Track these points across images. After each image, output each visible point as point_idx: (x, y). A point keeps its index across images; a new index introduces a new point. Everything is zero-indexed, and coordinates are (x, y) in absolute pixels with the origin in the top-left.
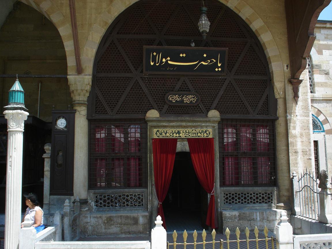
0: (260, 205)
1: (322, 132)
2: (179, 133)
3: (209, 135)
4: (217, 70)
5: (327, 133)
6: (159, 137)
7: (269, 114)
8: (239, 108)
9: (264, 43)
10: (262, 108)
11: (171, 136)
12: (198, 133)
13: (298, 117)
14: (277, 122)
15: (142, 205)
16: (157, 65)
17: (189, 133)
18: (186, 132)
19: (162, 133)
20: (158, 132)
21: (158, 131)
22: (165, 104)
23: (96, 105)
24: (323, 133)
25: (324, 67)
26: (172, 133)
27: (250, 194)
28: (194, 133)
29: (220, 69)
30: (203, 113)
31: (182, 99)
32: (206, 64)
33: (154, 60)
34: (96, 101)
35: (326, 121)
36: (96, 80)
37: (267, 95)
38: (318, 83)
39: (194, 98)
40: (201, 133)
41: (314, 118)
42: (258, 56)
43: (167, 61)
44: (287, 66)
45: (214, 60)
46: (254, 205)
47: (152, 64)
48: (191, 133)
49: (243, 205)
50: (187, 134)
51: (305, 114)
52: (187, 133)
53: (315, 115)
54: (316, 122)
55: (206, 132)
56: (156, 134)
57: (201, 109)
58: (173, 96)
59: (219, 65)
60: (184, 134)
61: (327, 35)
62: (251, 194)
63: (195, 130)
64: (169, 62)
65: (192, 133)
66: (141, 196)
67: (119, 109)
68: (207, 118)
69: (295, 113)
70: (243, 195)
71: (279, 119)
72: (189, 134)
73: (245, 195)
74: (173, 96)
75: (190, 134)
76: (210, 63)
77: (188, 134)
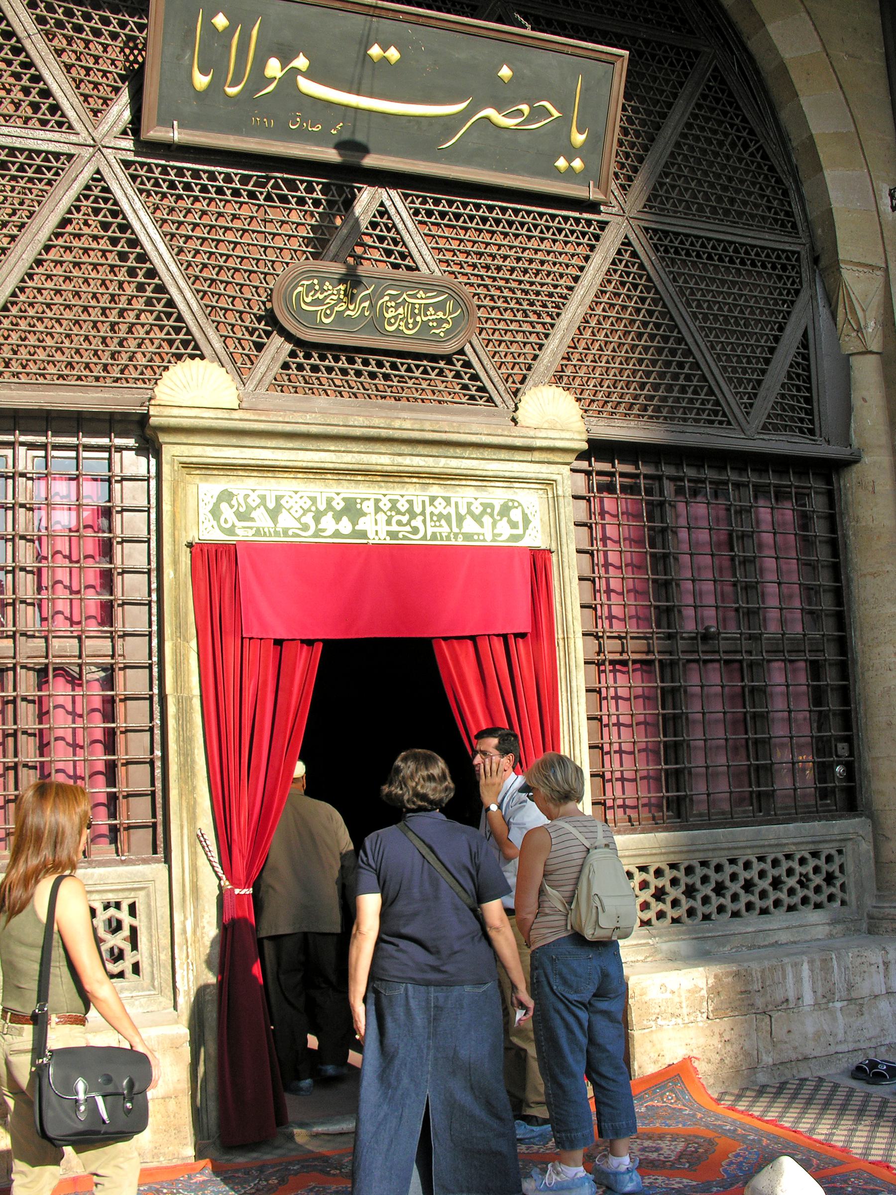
0: (793, 918)
2: (352, 510)
3: (526, 527)
4: (561, 163)
6: (231, 531)
7: (817, 431)
8: (676, 389)
9: (783, 69)
11: (306, 528)
12: (460, 519)
14: (850, 479)
15: (136, 969)
17: (413, 515)
18: (394, 507)
19: (250, 509)
20: (224, 506)
21: (226, 496)
22: (268, 334)
26: (309, 510)
27: (741, 864)
28: (440, 516)
29: (577, 164)
31: (372, 306)
39: (439, 307)
40: (478, 519)
42: (752, 132)
46: (765, 923)
48: (423, 513)
49: (709, 931)
50: (399, 523)
52: (399, 512)
55: (505, 510)
56: (215, 512)
57: (475, 377)
58: (321, 284)
59: (579, 139)
60: (382, 518)
62: (747, 866)
63: (447, 500)
64: (307, 86)
65: (432, 514)
66: (123, 915)
68: (516, 431)
70: (711, 872)
71: (866, 459)
72: (413, 523)
73: (719, 868)
74: (321, 284)
75: (417, 522)
76: (529, 120)
77: (405, 519)
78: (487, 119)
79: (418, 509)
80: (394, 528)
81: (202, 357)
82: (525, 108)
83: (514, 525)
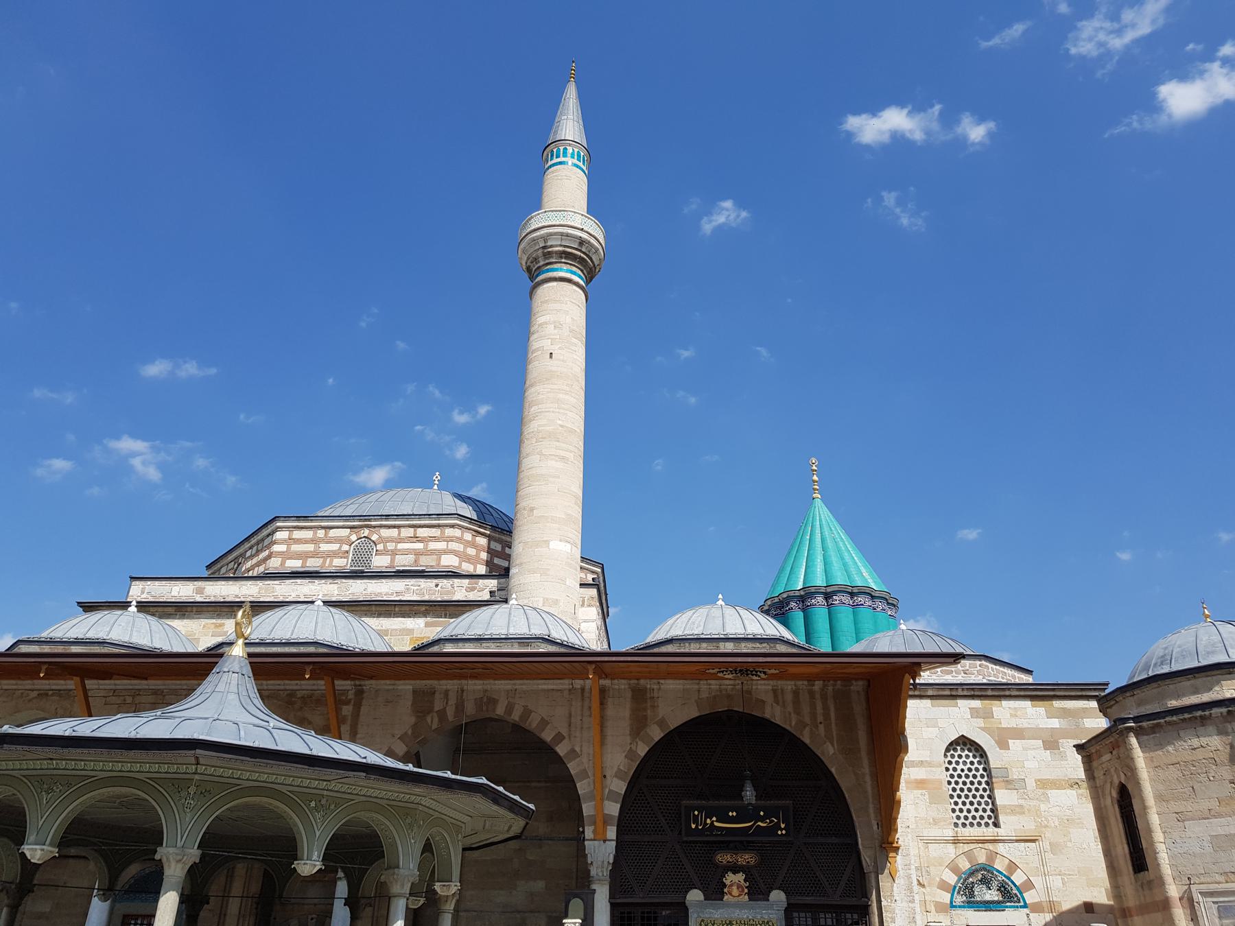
1: (1021, 907)
5: (1032, 912)
16: (700, 828)
21: (703, 921)
24: (1026, 911)
25: (1014, 774)
29: (784, 832)
32: (765, 825)
34: (621, 876)
35: (1029, 885)
38: (1005, 806)
41: (1003, 878)
43: (712, 822)
44: (878, 824)
45: (774, 819)
47: (693, 826)
53: (1004, 872)
55: (768, 923)
59: (783, 826)
63: (753, 920)
64: (716, 824)
76: (770, 823)
81: (696, 888)
82: (768, 821)
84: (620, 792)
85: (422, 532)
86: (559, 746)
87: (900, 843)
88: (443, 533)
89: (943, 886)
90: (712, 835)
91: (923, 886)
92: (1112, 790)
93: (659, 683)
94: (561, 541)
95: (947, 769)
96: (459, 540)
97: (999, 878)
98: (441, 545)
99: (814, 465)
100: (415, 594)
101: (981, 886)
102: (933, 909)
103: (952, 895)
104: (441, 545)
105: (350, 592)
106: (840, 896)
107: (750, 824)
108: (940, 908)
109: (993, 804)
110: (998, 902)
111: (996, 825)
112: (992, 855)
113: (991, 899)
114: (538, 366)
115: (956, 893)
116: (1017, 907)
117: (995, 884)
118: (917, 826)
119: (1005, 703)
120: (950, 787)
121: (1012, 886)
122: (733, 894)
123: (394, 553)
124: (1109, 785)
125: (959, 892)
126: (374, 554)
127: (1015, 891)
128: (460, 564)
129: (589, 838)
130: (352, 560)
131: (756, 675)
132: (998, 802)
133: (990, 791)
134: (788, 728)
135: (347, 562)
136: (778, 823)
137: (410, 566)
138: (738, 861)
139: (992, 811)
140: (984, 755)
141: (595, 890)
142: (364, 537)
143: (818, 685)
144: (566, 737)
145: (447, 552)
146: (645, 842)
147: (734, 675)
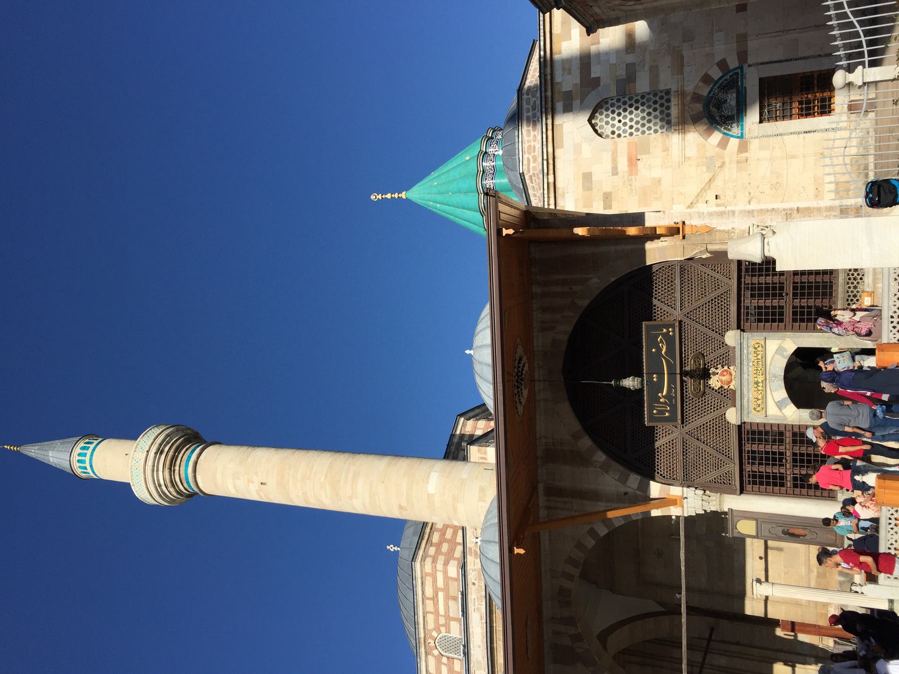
1: (742, 71)
4: (671, 333)
5: (746, 61)
10: (721, 273)
11: (761, 393)
12: (758, 359)
13: (735, 226)
16: (668, 408)
18: (756, 374)
19: (757, 404)
20: (757, 409)
21: (755, 409)
23: (721, 483)
24: (745, 66)
25: (622, 73)
27: (848, 290)
28: (757, 363)
29: (670, 329)
30: (729, 351)
33: (663, 412)
34: (715, 482)
36: (688, 482)
37: (703, 265)
40: (758, 355)
41: (716, 87)
43: (664, 397)
45: (659, 340)
47: (667, 414)
48: (757, 367)
50: (759, 373)
51: (730, 216)
53: (711, 86)
54: (724, 84)
55: (755, 348)
56: (758, 411)
59: (665, 330)
60: (758, 377)
61: (564, 69)
63: (753, 362)
64: (665, 393)
67: (726, 456)
68: (737, 347)
69: (729, 230)
70: (850, 299)
78: (665, 353)
79: (756, 369)
80: (760, 374)
81: (725, 414)
82: (660, 345)
83: (759, 346)
84: (639, 480)
85: (429, 592)
86: (599, 533)
87: (678, 221)
88: (428, 574)
89: (723, 145)
90: (676, 397)
91: (724, 163)
92: (628, 4)
93: (540, 438)
94: (428, 483)
95: (619, 136)
96: (434, 561)
97: (716, 91)
98: (440, 577)
99: (377, 197)
100: (481, 604)
101: (723, 109)
102: (744, 155)
103: (732, 136)
104: (440, 577)
105: (482, 660)
106: (730, 279)
107: (663, 360)
108: (743, 147)
109: (649, 94)
110: (738, 93)
111: (668, 92)
112: (696, 98)
113: (735, 100)
114: (274, 495)
115: (730, 133)
116: (742, 75)
117: (721, 96)
118: (669, 166)
119: (558, 79)
120: (635, 133)
121: (723, 79)
122: (729, 380)
123: (448, 618)
124: (622, 7)
125: (729, 130)
126: (450, 635)
127: (728, 77)
128: (455, 559)
129: (682, 512)
130: (455, 654)
131: (524, 366)
132: (648, 90)
133: (637, 96)
134: (577, 318)
135: (457, 659)
136: (663, 335)
137: (458, 603)
138: (699, 375)
139: (655, 95)
140: (605, 101)
141: (729, 509)
142: (435, 643)
143: (536, 289)
144: (591, 526)
145: (445, 572)
146: (684, 459)
147: (523, 387)
